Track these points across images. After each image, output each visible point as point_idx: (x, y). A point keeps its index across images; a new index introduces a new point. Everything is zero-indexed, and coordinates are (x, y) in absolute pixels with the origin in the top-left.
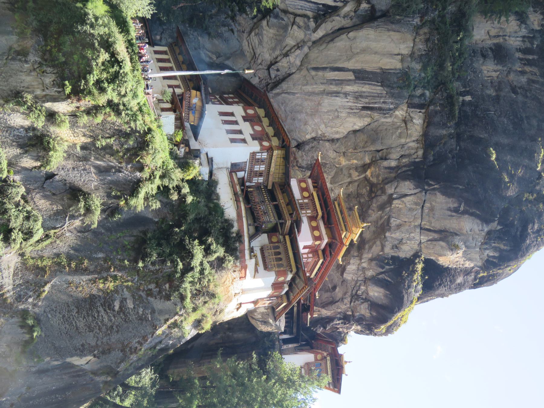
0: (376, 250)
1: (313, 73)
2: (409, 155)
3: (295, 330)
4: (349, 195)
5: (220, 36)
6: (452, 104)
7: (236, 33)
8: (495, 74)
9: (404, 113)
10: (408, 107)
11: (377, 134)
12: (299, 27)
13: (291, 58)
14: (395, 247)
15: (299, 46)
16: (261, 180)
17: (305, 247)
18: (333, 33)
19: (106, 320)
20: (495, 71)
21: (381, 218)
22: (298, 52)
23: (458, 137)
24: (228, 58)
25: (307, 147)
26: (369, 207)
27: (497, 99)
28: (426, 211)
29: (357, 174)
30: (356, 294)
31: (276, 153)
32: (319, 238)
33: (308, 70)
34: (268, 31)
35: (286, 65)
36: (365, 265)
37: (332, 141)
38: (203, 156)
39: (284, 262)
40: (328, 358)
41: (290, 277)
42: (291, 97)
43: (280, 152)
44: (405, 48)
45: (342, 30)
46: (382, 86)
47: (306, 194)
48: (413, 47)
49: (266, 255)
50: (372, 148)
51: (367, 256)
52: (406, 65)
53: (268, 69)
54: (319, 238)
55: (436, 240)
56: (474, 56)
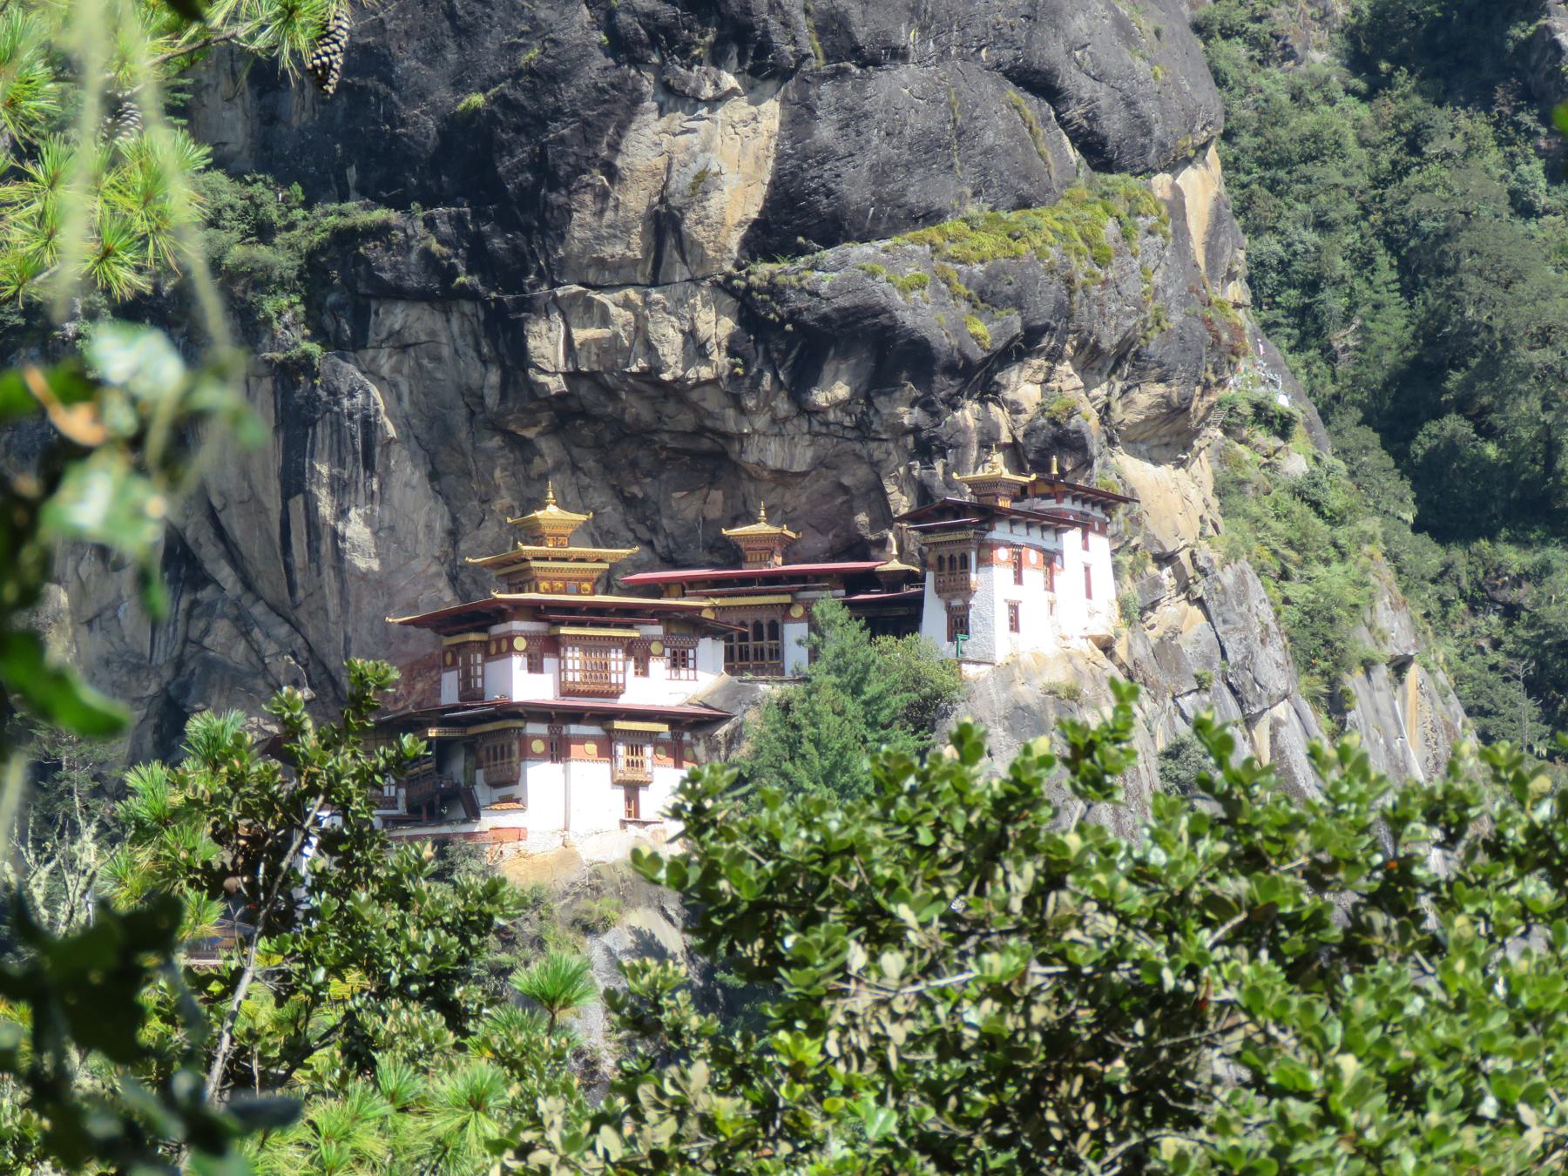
0: (712, 401)
1: (301, 594)
3: (902, 612)
4: (606, 467)
9: (385, 352)
10: (364, 347)
12: (206, 632)
21: (634, 390)
22: (257, 633)
26: (617, 422)
29: (537, 460)
33: (296, 607)
36: (761, 422)
37: (454, 535)
46: (314, 424)
50: (463, 435)
51: (730, 421)
54: (510, 638)
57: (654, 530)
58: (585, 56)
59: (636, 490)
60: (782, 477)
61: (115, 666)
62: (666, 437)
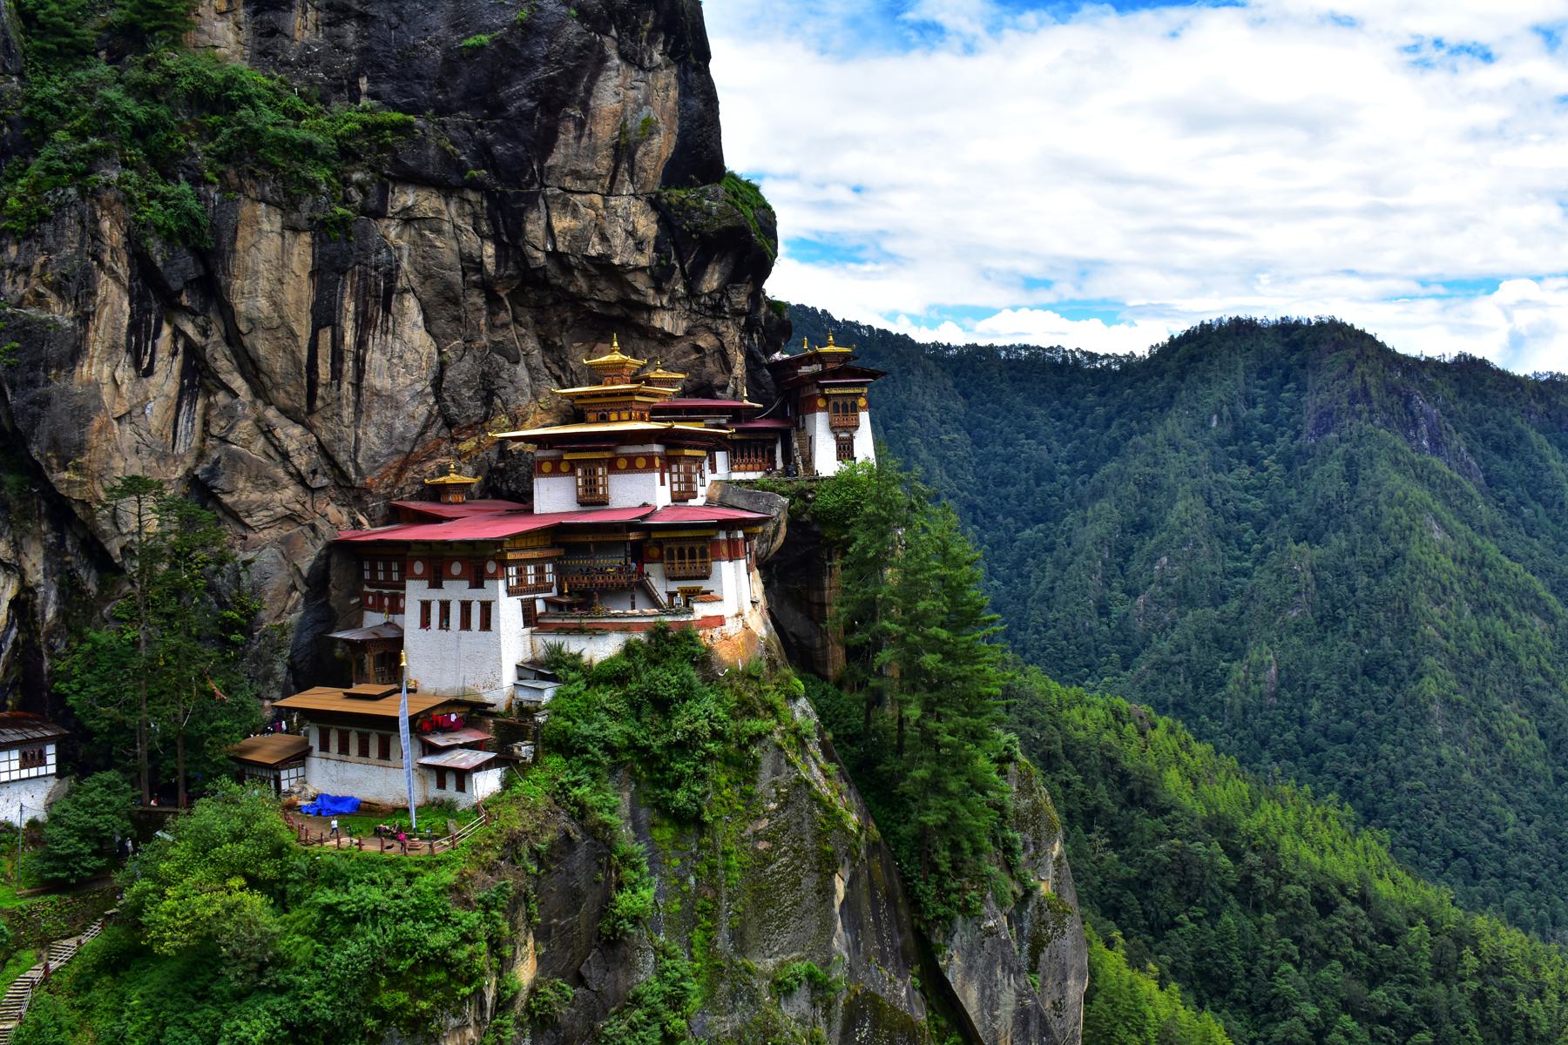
0: (641, 282)
1: (319, 403)
2: (476, 217)
4: (537, 322)
5: (257, 590)
6: (380, 126)
7: (250, 555)
8: (311, 15)
10: (384, 216)
11: (431, 276)
12: (231, 428)
13: (292, 446)
14: (639, 246)
15: (267, 431)
16: (549, 568)
17: (663, 483)
18: (236, 355)
19: (785, 860)
20: (305, 11)
21: (585, 272)
22: (279, 432)
23: (442, 110)
24: (299, 570)
25: (454, 410)
27: (364, 18)
28: (578, 185)
29: (503, 314)
30: (712, 308)
31: (510, 556)
32: (650, 459)
34: (243, 494)
35: (305, 458)
38: (524, 695)
39: (698, 547)
40: (827, 391)
41: (722, 536)
42: (363, 446)
43: (506, 545)
44: (271, 222)
45: (233, 338)
46: (344, 273)
47: (564, 467)
48: (268, 203)
49: (682, 573)
51: (652, 298)
52: (303, 224)
53: (313, 491)
55: (632, 166)
56: (275, 56)
57: (563, 369)
58: (562, 24)
59: (557, 340)
60: (668, 339)
61: (144, 453)
62: (594, 305)
